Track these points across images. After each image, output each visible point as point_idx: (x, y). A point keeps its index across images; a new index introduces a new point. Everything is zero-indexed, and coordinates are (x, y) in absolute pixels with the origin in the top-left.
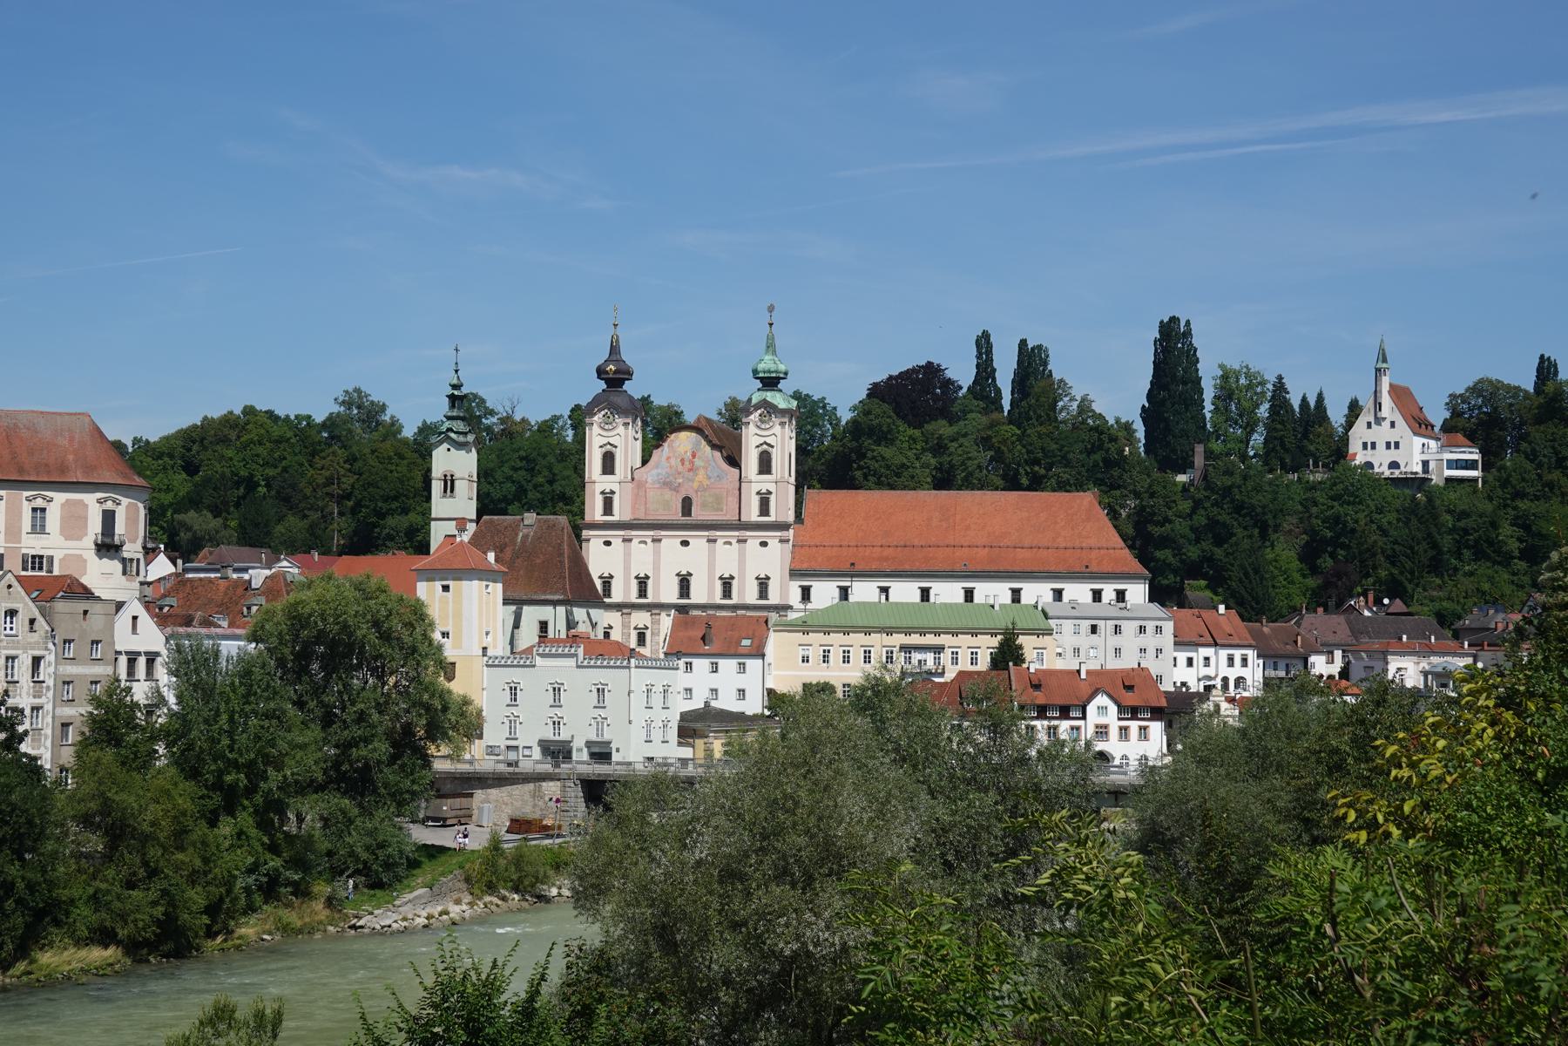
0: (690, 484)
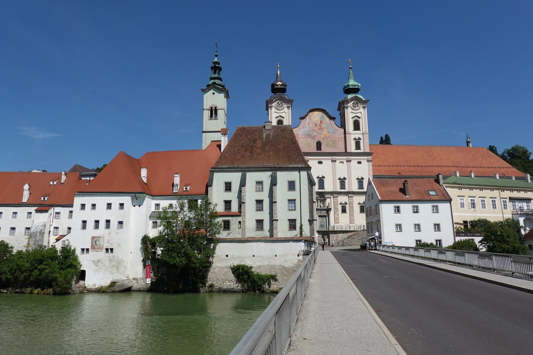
0: (320, 135)
